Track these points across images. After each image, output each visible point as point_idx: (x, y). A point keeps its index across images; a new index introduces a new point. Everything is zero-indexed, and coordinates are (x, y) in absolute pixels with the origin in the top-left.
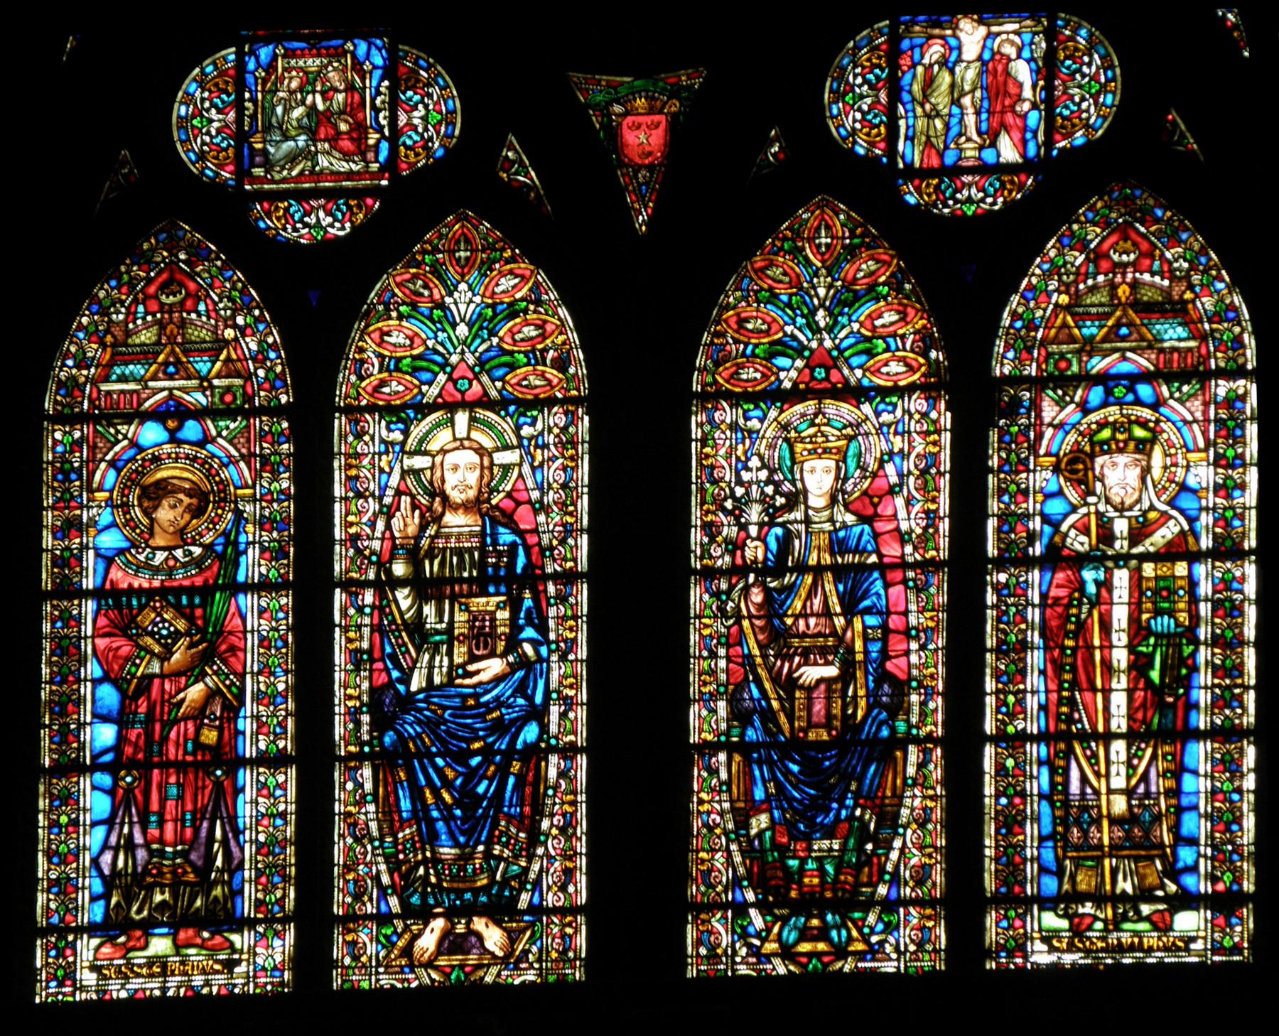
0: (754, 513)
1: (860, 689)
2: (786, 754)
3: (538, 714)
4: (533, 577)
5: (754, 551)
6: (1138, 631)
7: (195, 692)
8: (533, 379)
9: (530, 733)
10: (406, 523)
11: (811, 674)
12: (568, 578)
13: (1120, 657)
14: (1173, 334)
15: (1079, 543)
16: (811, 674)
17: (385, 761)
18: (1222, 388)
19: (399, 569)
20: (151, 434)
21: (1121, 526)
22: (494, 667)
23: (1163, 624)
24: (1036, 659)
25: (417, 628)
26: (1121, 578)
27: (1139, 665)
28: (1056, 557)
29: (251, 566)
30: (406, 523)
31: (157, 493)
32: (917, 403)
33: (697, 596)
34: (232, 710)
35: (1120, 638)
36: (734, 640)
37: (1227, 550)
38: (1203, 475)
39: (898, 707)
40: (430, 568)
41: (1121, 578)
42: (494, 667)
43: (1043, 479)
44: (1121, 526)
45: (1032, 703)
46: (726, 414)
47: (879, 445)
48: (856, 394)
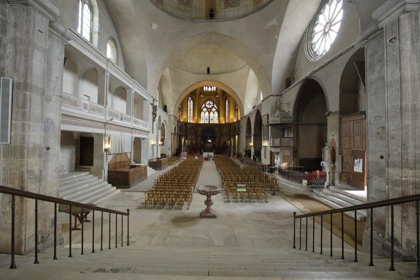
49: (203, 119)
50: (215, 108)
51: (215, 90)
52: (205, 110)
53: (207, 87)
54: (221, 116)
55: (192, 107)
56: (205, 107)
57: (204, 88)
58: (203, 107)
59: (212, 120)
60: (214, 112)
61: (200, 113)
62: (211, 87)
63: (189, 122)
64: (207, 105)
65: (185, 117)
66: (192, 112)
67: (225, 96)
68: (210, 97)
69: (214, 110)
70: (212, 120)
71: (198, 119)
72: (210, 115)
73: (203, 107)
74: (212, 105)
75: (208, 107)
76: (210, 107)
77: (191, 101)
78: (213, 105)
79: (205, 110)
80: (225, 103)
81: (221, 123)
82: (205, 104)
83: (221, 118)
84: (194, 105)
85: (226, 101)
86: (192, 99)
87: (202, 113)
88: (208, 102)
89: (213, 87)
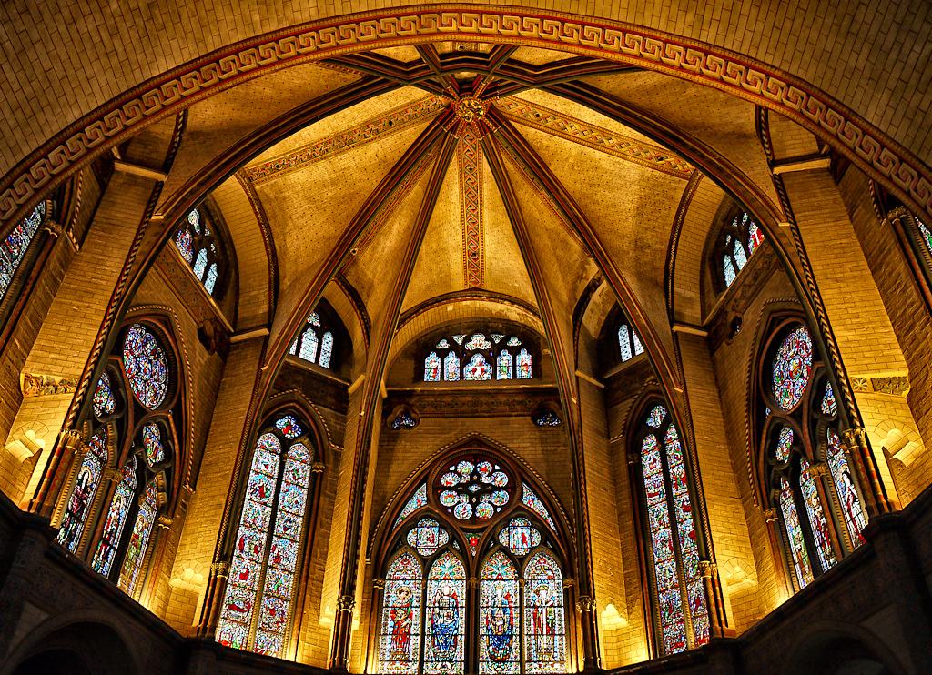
0: (490, 598)
1: (506, 625)
2: (495, 636)
3: (457, 629)
4: (457, 607)
5: (490, 604)
6: (547, 619)
7: (405, 623)
8: (457, 576)
9: (456, 632)
10: (438, 598)
11: (498, 624)
12: (462, 607)
13: (545, 623)
14: (550, 573)
15: (538, 604)
16: (498, 624)
17: (433, 636)
18: (557, 581)
19: (437, 605)
20: (401, 582)
21: (544, 602)
22: (450, 621)
23: (550, 617)
24: (532, 622)
25: (439, 614)
26: (544, 610)
27: (548, 624)
28: (535, 606)
29: (415, 604)
30: (438, 598)
31: (401, 592)
32: (514, 582)
33: (481, 610)
34: (410, 627)
35: (545, 619)
36: (487, 618)
37: (560, 606)
38: (555, 594)
39: (512, 629)
40: (441, 605)
41: (544, 610)
42: (450, 621)
43: (532, 594)
44: (544, 602)
45: (532, 629)
46: (486, 582)
47: (508, 588)
48: (504, 580)
49: (402, 635)
50: (535, 521)
51: (524, 373)
52: (427, 537)
53: (452, 360)
54: (600, 583)
55: (295, 499)
56: (444, 518)
57: (432, 361)
58: (411, 507)
59: (502, 639)
60: (518, 563)
61: (379, 570)
62: (491, 358)
63: (229, 633)
64: (446, 499)
65: (191, 574)
66: (289, 552)
67: (624, 410)
68: (483, 426)
69: (519, 537)
70: (502, 639)
71: (344, 620)
72: (487, 588)
73: (411, 507)
74: (502, 498)
75: (463, 510)
76: (486, 510)
77: (299, 451)
78: (512, 488)
79: (427, 537)
80: (636, 474)
81: (606, 661)
82: (437, 489)
83: (610, 618)
84: (318, 489)
85: (635, 449)
86: (309, 433)
87: (401, 584)
88: (466, 467)
89: (505, 359)
